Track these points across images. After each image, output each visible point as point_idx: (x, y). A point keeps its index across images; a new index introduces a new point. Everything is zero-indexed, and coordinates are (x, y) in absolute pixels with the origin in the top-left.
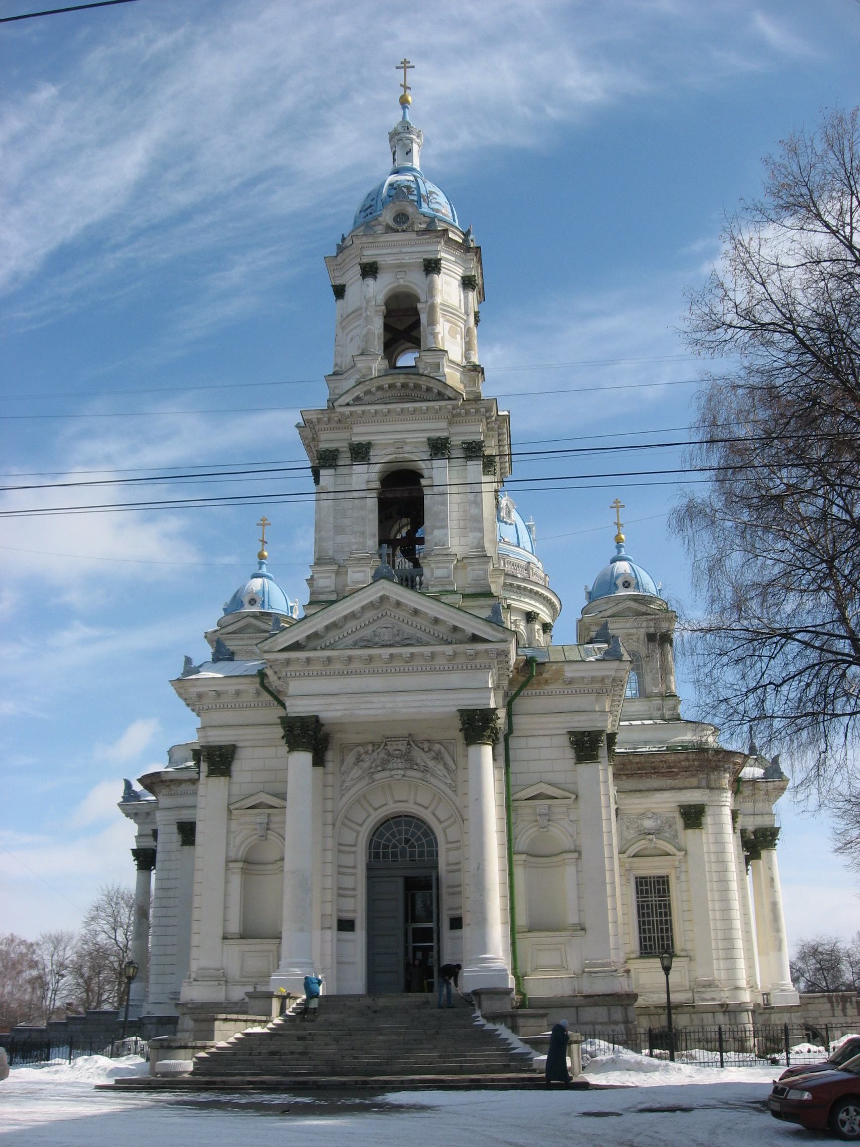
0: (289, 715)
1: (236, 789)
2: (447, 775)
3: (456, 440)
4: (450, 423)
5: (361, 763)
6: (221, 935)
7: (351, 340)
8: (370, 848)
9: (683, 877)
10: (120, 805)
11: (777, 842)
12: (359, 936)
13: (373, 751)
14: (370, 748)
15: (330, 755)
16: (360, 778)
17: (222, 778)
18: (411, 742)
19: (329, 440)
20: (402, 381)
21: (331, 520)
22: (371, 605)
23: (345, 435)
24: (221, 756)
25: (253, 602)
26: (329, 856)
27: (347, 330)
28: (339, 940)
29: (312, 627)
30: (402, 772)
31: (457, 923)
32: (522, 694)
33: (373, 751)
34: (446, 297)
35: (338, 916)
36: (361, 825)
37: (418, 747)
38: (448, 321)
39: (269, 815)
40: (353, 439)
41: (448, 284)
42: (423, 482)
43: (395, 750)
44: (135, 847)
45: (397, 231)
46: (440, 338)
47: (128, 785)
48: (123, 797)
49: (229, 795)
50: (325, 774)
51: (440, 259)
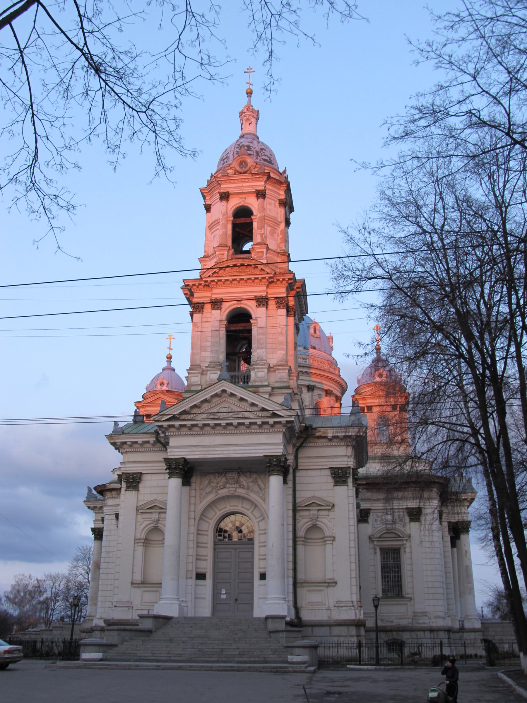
0: (169, 457)
1: (141, 497)
2: (260, 491)
4: (267, 287)
5: (212, 484)
6: (130, 580)
7: (214, 237)
8: (217, 532)
9: (408, 550)
11: (470, 529)
12: (209, 582)
16: (210, 492)
17: (134, 491)
19: (200, 296)
21: (199, 343)
22: (216, 395)
23: (208, 294)
24: (133, 478)
26: (192, 537)
27: (213, 231)
28: (196, 585)
30: (234, 489)
32: (304, 445)
34: (268, 212)
35: (196, 572)
36: (211, 519)
38: (270, 226)
39: (160, 513)
40: (213, 296)
41: (270, 204)
42: (252, 321)
44: (93, 527)
45: (241, 173)
47: (90, 489)
48: (87, 497)
49: (137, 501)
50: (190, 490)
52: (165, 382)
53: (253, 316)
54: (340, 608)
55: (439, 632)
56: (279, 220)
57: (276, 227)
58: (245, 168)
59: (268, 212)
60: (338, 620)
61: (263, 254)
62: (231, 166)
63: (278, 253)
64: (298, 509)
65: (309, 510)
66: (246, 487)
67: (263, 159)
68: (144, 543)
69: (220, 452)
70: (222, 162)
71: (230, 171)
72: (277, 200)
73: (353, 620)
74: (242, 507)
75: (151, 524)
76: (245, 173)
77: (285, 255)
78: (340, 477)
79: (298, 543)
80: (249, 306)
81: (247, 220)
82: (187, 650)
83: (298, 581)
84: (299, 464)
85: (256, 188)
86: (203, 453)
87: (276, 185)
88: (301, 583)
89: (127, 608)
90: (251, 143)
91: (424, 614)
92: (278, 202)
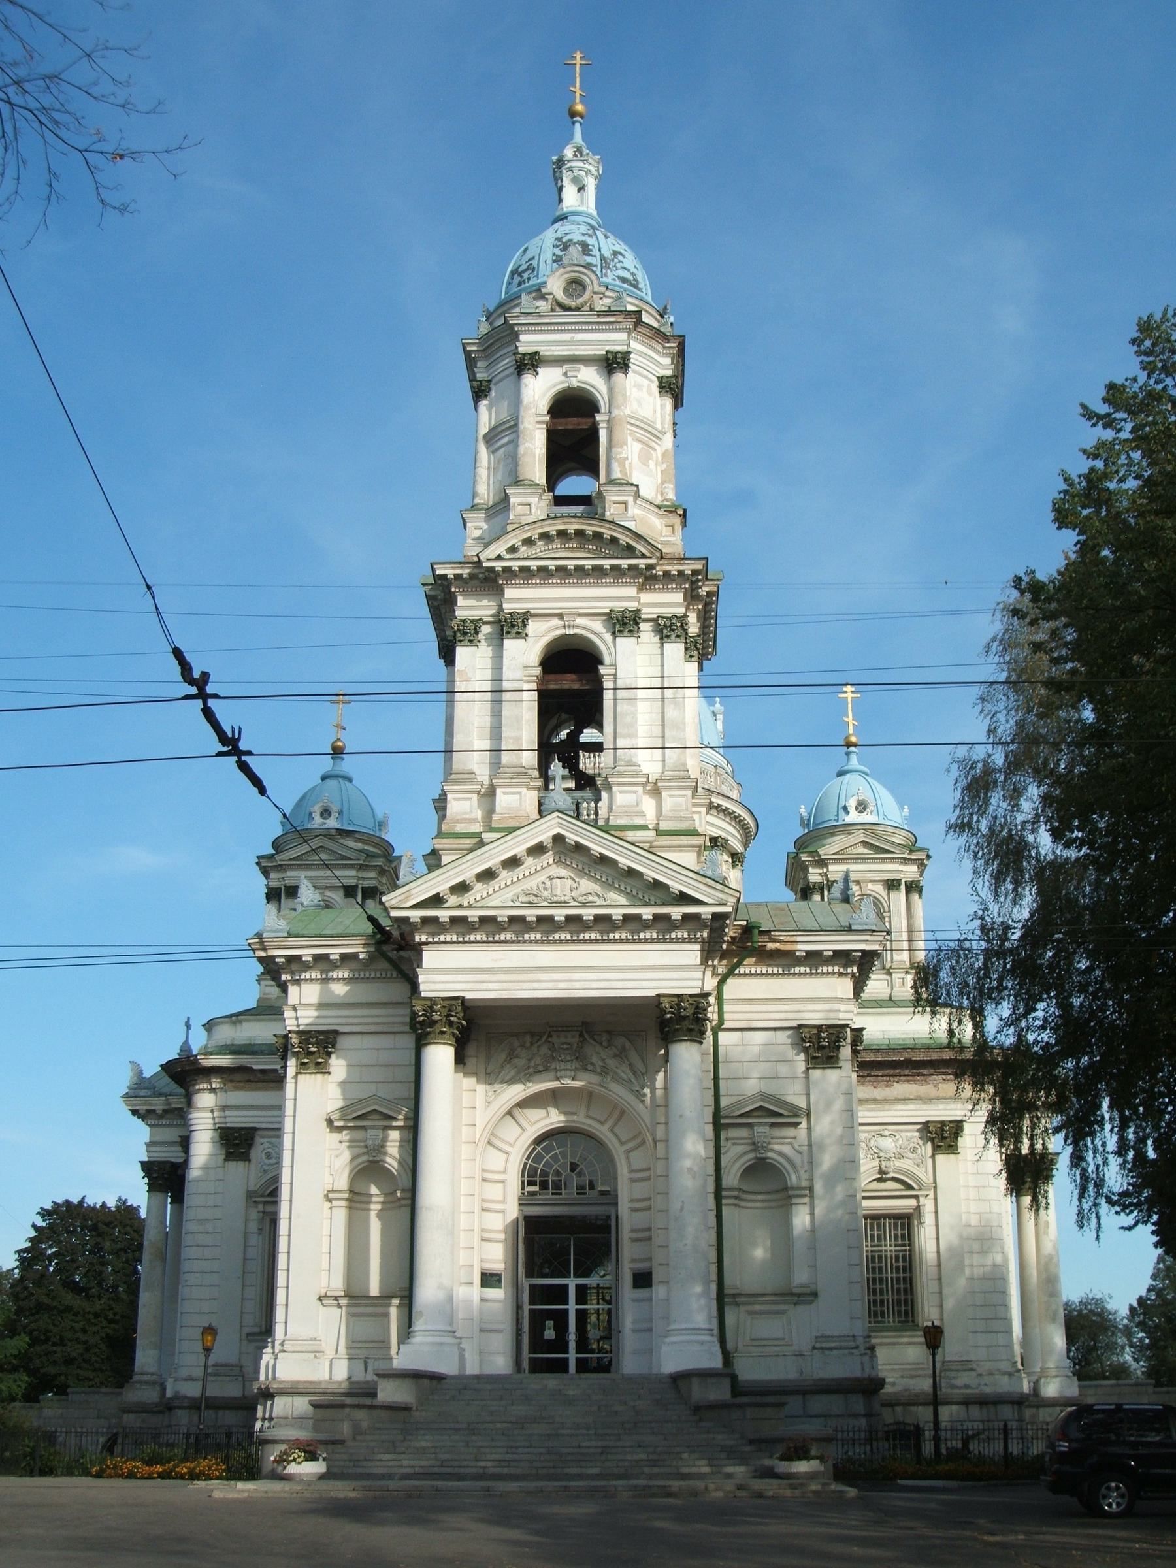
3: (647, 613)
5: (516, 1061)
10: (126, 1096)
11: (1054, 1172)
13: (532, 1044)
14: (528, 1039)
15: (471, 1050)
18: (586, 1036)
20: (577, 527)
25: (326, 815)
29: (458, 874)
31: (643, 1280)
32: (736, 972)
33: (532, 1044)
37: (595, 1040)
41: (639, 387)
43: (563, 1044)
44: (146, 1159)
45: (569, 309)
46: (627, 466)
51: (629, 353)
52: (334, 808)
53: (607, 660)
54: (827, 1352)
55: (999, 1407)
56: (659, 426)
57: (653, 444)
58: (580, 296)
59: (635, 405)
60: (822, 1380)
61: (626, 509)
62: (544, 290)
63: (659, 507)
64: (723, 1121)
65: (750, 1126)
66: (599, 1070)
67: (618, 277)
68: (347, 1200)
69: (550, 985)
70: (517, 279)
71: (543, 305)
72: (656, 379)
73: (857, 1379)
74: (589, 1117)
75: (745, 1153)
76: (578, 309)
77: (675, 512)
78: (824, 1047)
79: (724, 1201)
80: (595, 633)
81: (584, 424)
82: (520, 1450)
83: (726, 1291)
84: (726, 1016)
85: (608, 348)
86: (505, 986)
87: (653, 343)
88: (734, 1296)
89: (313, 1355)
90: (590, 235)
91: (966, 1365)
92: (657, 383)
